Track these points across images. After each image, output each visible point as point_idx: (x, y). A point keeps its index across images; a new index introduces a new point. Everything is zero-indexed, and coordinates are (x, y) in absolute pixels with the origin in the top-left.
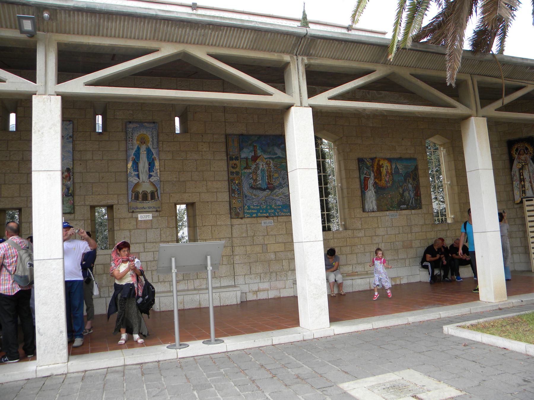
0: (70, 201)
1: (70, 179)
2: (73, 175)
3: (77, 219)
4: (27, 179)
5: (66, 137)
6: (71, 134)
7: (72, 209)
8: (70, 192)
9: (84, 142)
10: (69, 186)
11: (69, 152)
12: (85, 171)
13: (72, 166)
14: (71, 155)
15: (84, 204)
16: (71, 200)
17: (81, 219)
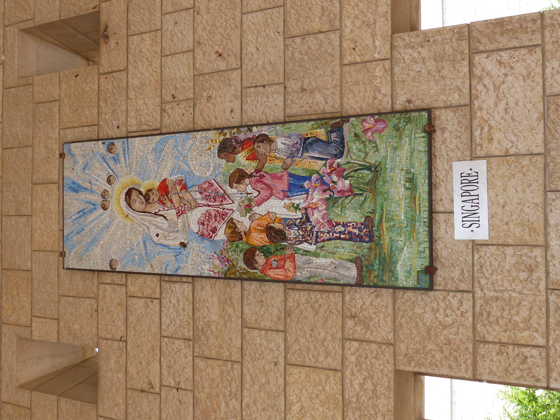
0: (365, 131)
1: (264, 139)
2: (249, 127)
3: (466, 91)
4: (267, 330)
5: (111, 162)
6: (101, 147)
7: (408, 121)
8: (321, 133)
9: (132, 94)
10: (295, 139)
11: (158, 150)
12: (235, 75)
13: (212, 134)
14: (171, 140)
15: (387, 64)
16: (359, 130)
17: (466, 69)
